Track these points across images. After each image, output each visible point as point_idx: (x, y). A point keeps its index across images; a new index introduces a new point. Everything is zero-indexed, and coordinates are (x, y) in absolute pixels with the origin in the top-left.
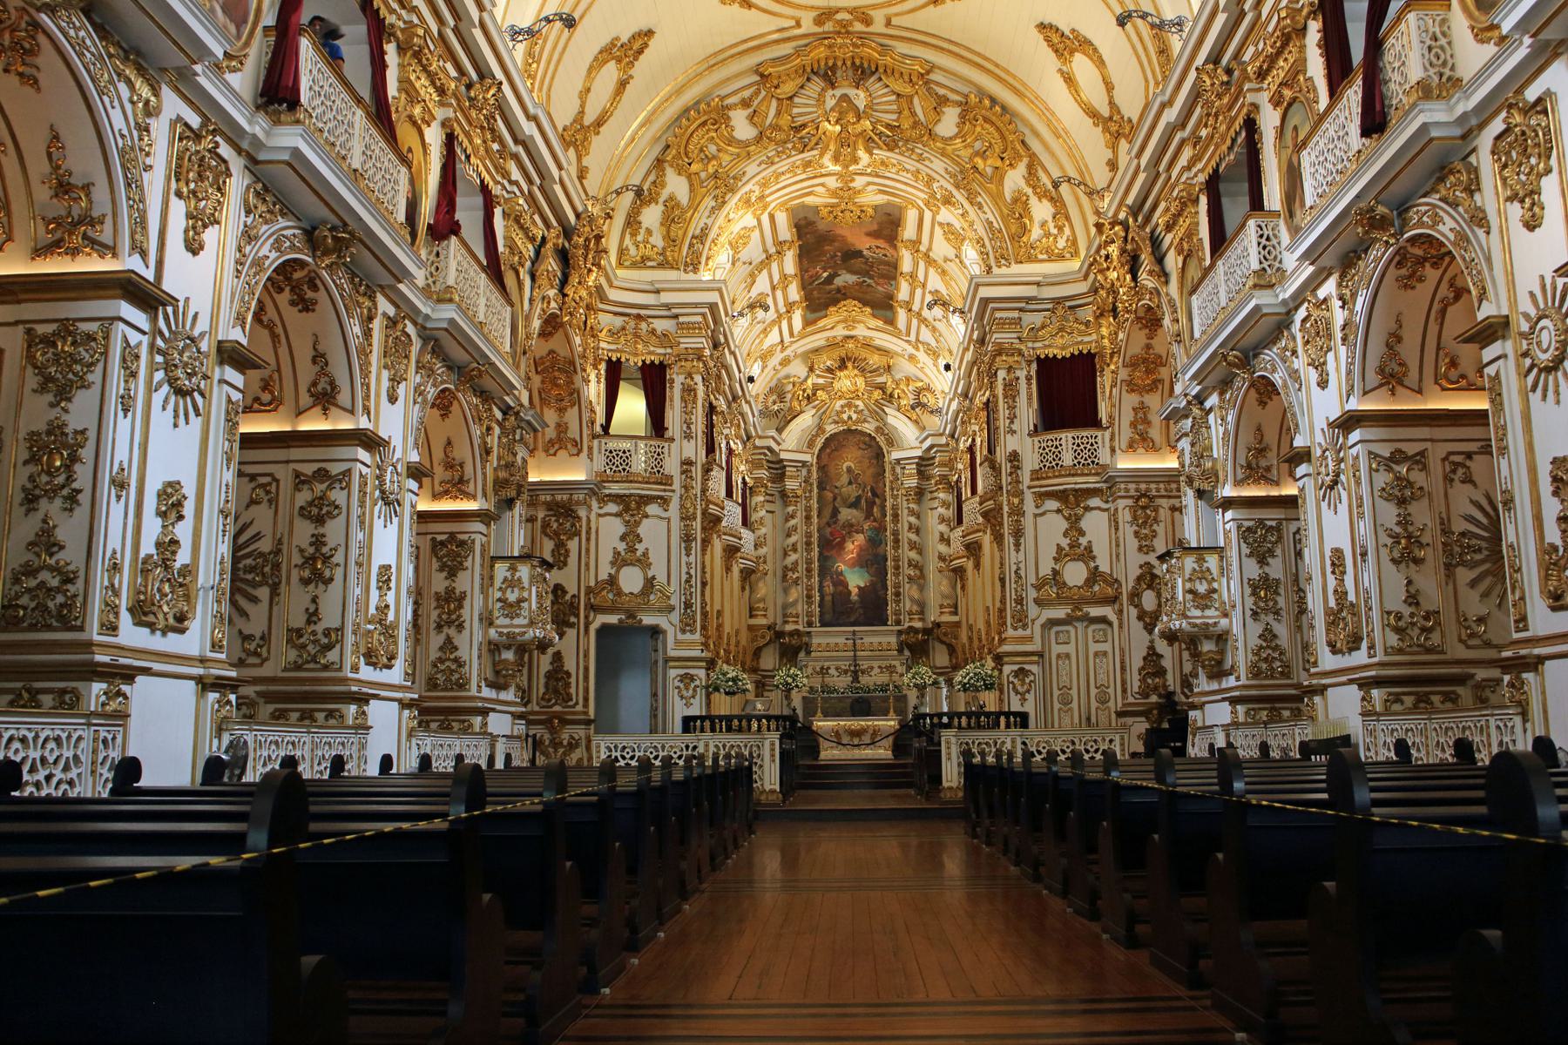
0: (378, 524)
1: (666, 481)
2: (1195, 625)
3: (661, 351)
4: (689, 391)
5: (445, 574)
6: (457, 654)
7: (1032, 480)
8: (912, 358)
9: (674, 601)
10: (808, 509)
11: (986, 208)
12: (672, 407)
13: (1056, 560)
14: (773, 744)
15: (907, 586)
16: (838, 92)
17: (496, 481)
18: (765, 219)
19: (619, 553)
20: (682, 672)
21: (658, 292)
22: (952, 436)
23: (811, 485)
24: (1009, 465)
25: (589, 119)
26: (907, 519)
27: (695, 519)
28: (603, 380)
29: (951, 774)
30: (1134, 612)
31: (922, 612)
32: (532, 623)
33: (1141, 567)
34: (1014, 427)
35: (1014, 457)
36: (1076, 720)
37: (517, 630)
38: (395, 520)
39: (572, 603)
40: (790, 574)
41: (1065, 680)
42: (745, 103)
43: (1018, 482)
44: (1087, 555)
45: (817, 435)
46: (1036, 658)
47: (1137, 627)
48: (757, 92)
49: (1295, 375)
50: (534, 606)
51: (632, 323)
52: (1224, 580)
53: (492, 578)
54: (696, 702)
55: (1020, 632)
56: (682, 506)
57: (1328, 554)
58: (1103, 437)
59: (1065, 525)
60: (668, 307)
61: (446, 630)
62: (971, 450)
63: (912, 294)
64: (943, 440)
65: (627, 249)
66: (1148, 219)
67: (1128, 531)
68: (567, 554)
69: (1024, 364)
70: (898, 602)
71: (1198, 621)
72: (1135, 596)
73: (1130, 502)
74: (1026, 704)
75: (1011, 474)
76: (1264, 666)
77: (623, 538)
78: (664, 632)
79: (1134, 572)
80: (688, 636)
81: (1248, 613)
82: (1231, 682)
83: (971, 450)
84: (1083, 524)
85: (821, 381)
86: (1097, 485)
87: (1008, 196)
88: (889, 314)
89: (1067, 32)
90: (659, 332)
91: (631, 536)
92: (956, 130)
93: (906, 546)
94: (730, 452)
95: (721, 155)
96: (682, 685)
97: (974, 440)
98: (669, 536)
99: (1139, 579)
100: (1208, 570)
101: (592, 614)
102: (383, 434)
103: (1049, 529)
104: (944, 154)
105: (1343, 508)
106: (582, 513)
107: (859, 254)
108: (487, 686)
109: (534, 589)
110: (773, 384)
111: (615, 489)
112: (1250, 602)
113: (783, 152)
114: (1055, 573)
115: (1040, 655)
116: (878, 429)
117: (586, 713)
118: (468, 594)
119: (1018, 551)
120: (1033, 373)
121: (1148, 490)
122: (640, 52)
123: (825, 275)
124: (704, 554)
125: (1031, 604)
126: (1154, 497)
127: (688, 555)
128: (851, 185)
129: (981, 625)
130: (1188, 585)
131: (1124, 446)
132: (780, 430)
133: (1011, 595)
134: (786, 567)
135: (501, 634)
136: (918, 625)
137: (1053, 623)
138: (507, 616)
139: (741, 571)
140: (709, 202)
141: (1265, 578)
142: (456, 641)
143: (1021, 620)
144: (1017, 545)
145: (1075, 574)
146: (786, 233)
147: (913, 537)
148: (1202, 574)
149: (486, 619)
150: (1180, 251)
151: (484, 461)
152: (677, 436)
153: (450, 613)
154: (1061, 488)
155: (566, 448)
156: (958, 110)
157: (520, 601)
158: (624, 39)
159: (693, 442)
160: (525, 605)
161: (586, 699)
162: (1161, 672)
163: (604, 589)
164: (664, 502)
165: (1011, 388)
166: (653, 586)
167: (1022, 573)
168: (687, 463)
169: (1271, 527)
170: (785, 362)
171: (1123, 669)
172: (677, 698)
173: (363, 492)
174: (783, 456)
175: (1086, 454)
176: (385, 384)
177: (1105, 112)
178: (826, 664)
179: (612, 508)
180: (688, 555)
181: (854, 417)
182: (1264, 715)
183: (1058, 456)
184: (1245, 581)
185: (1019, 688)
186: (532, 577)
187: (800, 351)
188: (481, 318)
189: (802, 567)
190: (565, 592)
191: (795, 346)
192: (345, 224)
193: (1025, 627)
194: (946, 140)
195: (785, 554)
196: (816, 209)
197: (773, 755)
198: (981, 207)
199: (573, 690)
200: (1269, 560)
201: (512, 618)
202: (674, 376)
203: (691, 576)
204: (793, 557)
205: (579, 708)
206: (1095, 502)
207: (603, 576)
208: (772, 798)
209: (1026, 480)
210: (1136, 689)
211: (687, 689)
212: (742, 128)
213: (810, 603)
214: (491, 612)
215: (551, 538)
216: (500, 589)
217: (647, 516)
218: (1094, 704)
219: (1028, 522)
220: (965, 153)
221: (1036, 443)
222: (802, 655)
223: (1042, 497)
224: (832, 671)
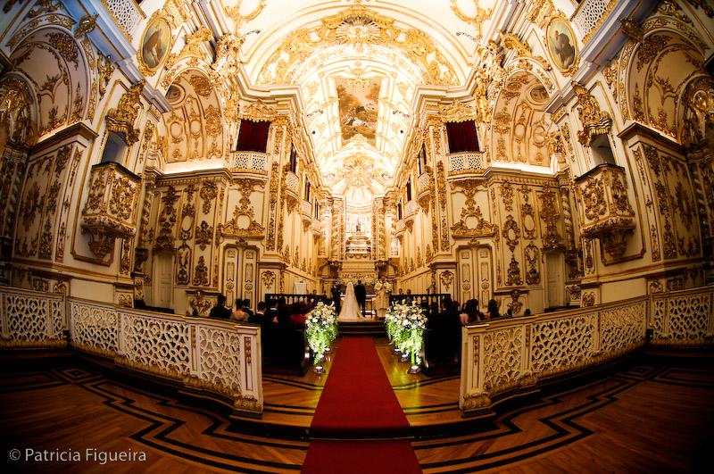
1: (265, 174)
8: (381, 161)
13: (463, 216)
18: (324, 79)
20: (266, 270)
26: (379, 220)
30: (505, 241)
35: (440, 165)
41: (466, 278)
43: (443, 177)
44: (477, 213)
46: (454, 266)
47: (507, 248)
55: (445, 252)
59: (465, 199)
60: (273, 97)
64: (393, 189)
67: (499, 199)
72: (505, 232)
73: (500, 185)
77: (241, 201)
79: (504, 220)
80: (270, 252)
84: (475, 198)
91: (245, 201)
99: (507, 223)
103: (458, 201)
106: (219, 186)
107: (362, 109)
111: (239, 176)
114: (462, 222)
115: (455, 263)
117: (217, 290)
125: (451, 237)
128: (360, 67)
136: (383, 260)
137: (461, 248)
143: (446, 245)
144: (443, 207)
145: (472, 223)
146: (334, 94)
162: (517, 272)
171: (499, 270)
172: (263, 285)
190: (207, 226)
195: (333, 233)
196: (345, 80)
199: (208, 277)
204: (336, 233)
207: (229, 219)
209: (447, 178)
212: (314, 37)
217: (254, 191)
218: (481, 289)
222: (338, 271)
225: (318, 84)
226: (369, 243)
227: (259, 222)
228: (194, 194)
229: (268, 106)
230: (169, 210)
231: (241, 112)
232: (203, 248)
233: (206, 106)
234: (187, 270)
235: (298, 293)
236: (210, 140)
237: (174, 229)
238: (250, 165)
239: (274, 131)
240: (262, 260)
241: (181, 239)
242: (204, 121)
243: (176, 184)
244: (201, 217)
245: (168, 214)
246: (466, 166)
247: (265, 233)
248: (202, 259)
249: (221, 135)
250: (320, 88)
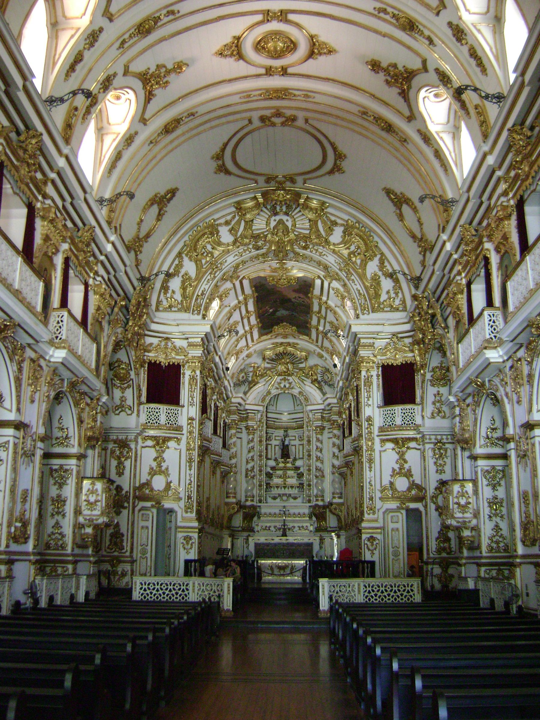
0: (23, 467)
1: (179, 429)
2: (458, 522)
5: (57, 487)
6: (62, 530)
7: (379, 432)
9: (182, 495)
10: (261, 437)
11: (356, 282)
14: (229, 584)
15: (315, 481)
16: (278, 218)
17: (85, 435)
18: (237, 284)
19: (152, 469)
22: (341, 399)
23: (263, 423)
24: (366, 423)
25: (142, 235)
26: (314, 443)
27: (194, 450)
29: (324, 604)
30: (433, 506)
31: (323, 496)
32: (102, 514)
33: (437, 481)
34: (370, 402)
35: (369, 419)
36: (402, 565)
37: (94, 518)
38: (31, 465)
39: (126, 496)
40: (249, 473)
42: (227, 223)
43: (371, 433)
44: (408, 474)
45: (267, 395)
46: (380, 531)
48: (234, 217)
49: (507, 394)
50: (104, 505)
52: (475, 497)
53: (81, 488)
54: (192, 551)
56: (188, 443)
57: (521, 493)
58: (417, 408)
59: (397, 457)
61: (56, 517)
62: (350, 408)
63: (319, 322)
64: (335, 401)
65: (161, 301)
66: (439, 297)
67: (430, 462)
69: (375, 368)
70: (310, 490)
71: (460, 520)
72: (434, 497)
73: (432, 446)
74: (374, 556)
75: (367, 428)
76: (494, 545)
77: (155, 460)
78: (176, 512)
80: (189, 514)
81: (486, 517)
82: (476, 553)
83: (350, 408)
84: (407, 457)
85: (269, 366)
86: (415, 436)
87: (369, 276)
88: (307, 331)
89: (398, 194)
90: (178, 348)
91: (160, 459)
92: (341, 240)
93: (315, 459)
94: (216, 407)
95: (214, 251)
96: (185, 542)
97: (351, 404)
98: (180, 458)
100: (466, 492)
101: (137, 502)
102: (26, 421)
104: (334, 251)
105: (528, 469)
106: (133, 446)
107: (290, 300)
108: (77, 547)
109: (104, 495)
110: (242, 367)
111: (152, 433)
112: (487, 510)
113: (247, 250)
114: (391, 483)
115: (383, 528)
116: (300, 393)
117: (131, 557)
118: (69, 498)
119: (370, 471)
120: (380, 373)
121: (442, 439)
122: (171, 198)
123: (271, 311)
125: (377, 499)
126: (445, 443)
127: (190, 470)
129: (353, 507)
130: (456, 500)
131: (429, 415)
132: (245, 393)
133: (366, 496)
134: (247, 469)
135: (85, 519)
136: (320, 503)
138: (89, 509)
139: (222, 473)
140: (207, 276)
141: (495, 497)
142: (61, 524)
143: (372, 509)
144: (370, 468)
146: (248, 290)
147: (319, 454)
148: (463, 494)
149: (78, 512)
150: (454, 317)
151: (79, 427)
152: (186, 404)
153: (58, 508)
154: (394, 437)
155: (125, 411)
156: (342, 229)
157: (96, 501)
158: (162, 193)
159: (194, 407)
160: (99, 504)
161: (132, 549)
164: (178, 440)
165: (368, 382)
166: (170, 487)
167: (373, 483)
168: (192, 419)
169: (499, 470)
170: (248, 356)
172: (182, 549)
173: (15, 453)
174: (247, 407)
175: (408, 418)
176: (30, 393)
177: (419, 235)
178: (268, 525)
179: (150, 443)
180: (190, 470)
181: (287, 386)
182: (494, 573)
183: (393, 419)
184: (485, 499)
185: (371, 548)
186: (103, 489)
187: (257, 349)
188: (80, 353)
189: (256, 470)
190: (122, 489)
191: (254, 347)
192: (11, 318)
193: (374, 513)
194: (334, 244)
196: (265, 278)
197: (229, 590)
198: (354, 282)
199: (125, 544)
200: (498, 488)
201: (92, 510)
203: (191, 482)
205: (128, 554)
206: (412, 444)
207: (143, 481)
208: (228, 614)
210: (434, 549)
211: (188, 544)
212: (226, 236)
213: (260, 490)
214: (80, 507)
216: (86, 494)
217: (168, 448)
219: (377, 455)
220: (345, 252)
221: (382, 413)
222: (255, 519)
223: (383, 441)
224: (272, 529)
226: (300, 476)
236: (117, 393)
238: (163, 420)
246: (398, 421)
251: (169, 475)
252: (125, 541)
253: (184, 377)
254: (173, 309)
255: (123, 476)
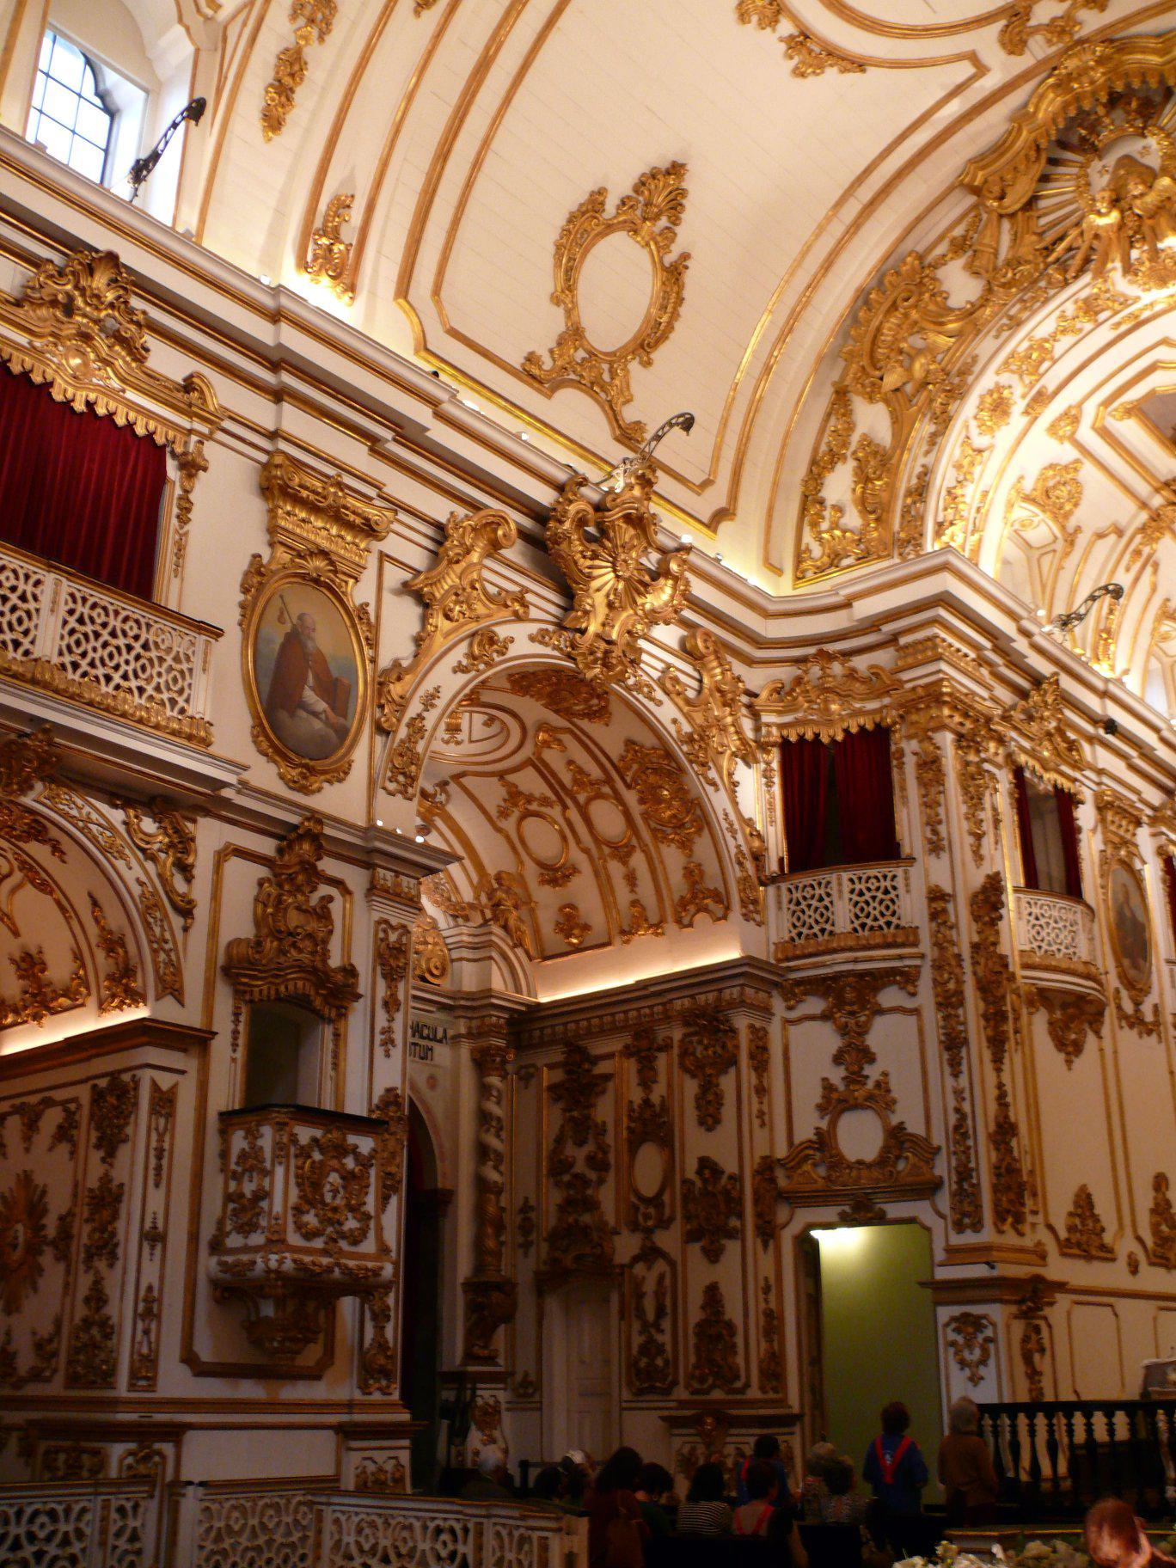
1: (909, 937)
3: (872, 705)
4: (930, 766)
5: (101, 1153)
12: (905, 798)
16: (1111, 159)
20: (957, 1310)
21: (847, 604)
28: (777, 780)
51: (816, 671)
54: (988, 1372)
60: (873, 624)
65: (808, 550)
68: (719, 1098)
77: (838, 1059)
80: (969, 1238)
91: (855, 1054)
96: (960, 1339)
106: (742, 1022)
117: (783, 1402)
124: (998, 1070)
140: (925, 428)
155: (706, 910)
159: (945, 856)
163: (807, 1157)
172: (954, 1367)
179: (814, 1005)
199: (740, 1360)
202: (904, 744)
207: (805, 1130)
212: (960, 285)
215: (693, 1076)
217: (881, 1011)
225: (1074, 466)
227: (915, 1127)
228: (662, 1061)
229: (861, 663)
230: (581, 1127)
231: (766, 718)
232: (713, 1255)
233: (615, 750)
234: (665, 1339)
235: (1067, 1396)
237: (607, 1198)
238: (843, 916)
239: (910, 762)
240: (942, 1274)
241: (635, 1227)
242: (631, 797)
243: (590, 1034)
244: (696, 1144)
245: (580, 1143)
247: (942, 1167)
248: (713, 1295)
249: (706, 832)
250: (1088, 472)
251: (890, 1105)
252: (692, 1350)
253: (901, 766)
254: (845, 562)
255: (719, 1129)
